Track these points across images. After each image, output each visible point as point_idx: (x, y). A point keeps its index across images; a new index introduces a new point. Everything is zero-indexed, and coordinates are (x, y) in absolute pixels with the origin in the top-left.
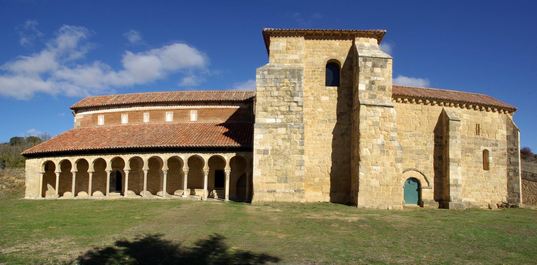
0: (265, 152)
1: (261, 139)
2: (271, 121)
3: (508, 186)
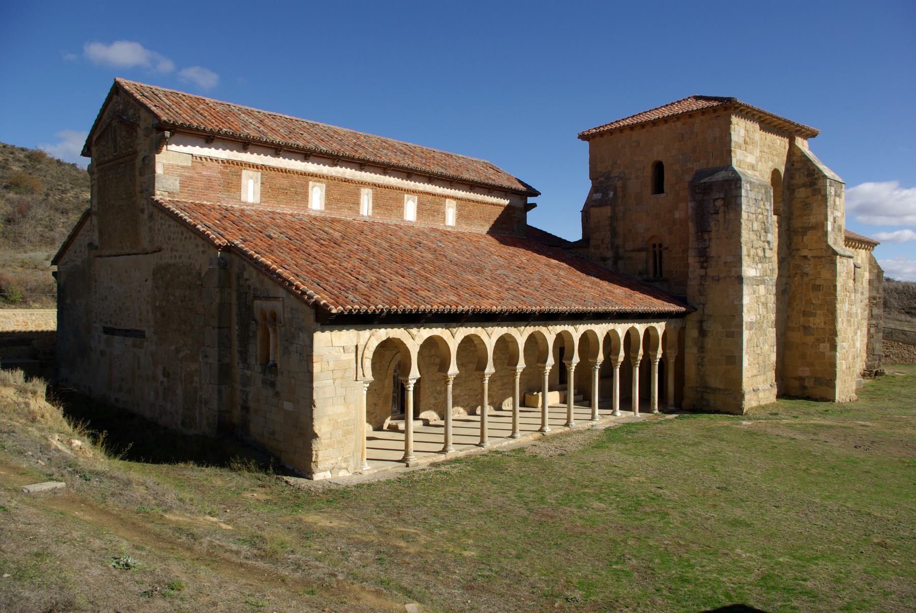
3: (867, 348)
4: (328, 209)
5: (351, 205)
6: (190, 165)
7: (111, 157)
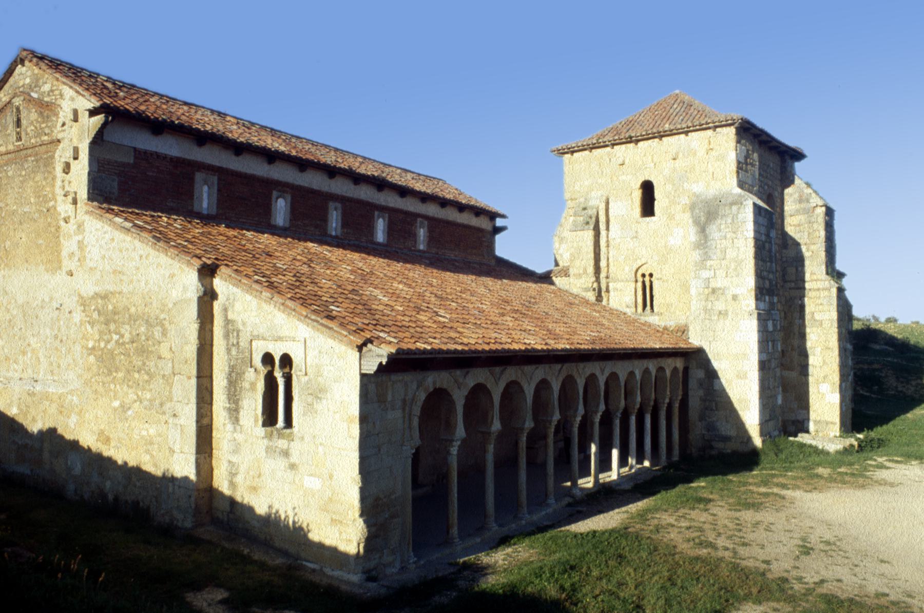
5: (318, 222)
6: (132, 161)
7: (11, 147)
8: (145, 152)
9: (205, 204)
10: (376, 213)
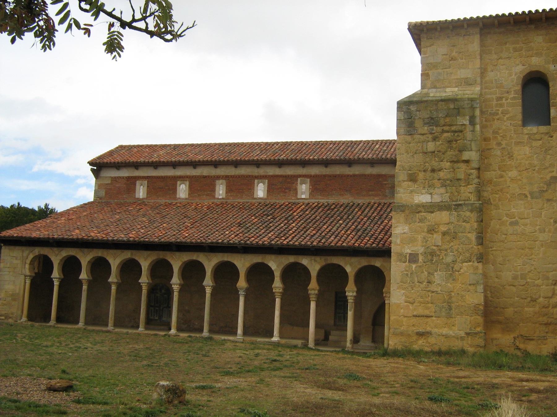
0: (413, 258)
1: (404, 233)
2: (424, 198)
4: (191, 197)
5: (209, 193)
8: (115, 177)
9: (141, 194)
10: (256, 181)
